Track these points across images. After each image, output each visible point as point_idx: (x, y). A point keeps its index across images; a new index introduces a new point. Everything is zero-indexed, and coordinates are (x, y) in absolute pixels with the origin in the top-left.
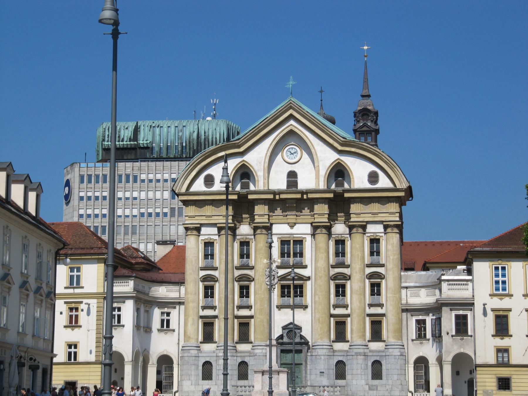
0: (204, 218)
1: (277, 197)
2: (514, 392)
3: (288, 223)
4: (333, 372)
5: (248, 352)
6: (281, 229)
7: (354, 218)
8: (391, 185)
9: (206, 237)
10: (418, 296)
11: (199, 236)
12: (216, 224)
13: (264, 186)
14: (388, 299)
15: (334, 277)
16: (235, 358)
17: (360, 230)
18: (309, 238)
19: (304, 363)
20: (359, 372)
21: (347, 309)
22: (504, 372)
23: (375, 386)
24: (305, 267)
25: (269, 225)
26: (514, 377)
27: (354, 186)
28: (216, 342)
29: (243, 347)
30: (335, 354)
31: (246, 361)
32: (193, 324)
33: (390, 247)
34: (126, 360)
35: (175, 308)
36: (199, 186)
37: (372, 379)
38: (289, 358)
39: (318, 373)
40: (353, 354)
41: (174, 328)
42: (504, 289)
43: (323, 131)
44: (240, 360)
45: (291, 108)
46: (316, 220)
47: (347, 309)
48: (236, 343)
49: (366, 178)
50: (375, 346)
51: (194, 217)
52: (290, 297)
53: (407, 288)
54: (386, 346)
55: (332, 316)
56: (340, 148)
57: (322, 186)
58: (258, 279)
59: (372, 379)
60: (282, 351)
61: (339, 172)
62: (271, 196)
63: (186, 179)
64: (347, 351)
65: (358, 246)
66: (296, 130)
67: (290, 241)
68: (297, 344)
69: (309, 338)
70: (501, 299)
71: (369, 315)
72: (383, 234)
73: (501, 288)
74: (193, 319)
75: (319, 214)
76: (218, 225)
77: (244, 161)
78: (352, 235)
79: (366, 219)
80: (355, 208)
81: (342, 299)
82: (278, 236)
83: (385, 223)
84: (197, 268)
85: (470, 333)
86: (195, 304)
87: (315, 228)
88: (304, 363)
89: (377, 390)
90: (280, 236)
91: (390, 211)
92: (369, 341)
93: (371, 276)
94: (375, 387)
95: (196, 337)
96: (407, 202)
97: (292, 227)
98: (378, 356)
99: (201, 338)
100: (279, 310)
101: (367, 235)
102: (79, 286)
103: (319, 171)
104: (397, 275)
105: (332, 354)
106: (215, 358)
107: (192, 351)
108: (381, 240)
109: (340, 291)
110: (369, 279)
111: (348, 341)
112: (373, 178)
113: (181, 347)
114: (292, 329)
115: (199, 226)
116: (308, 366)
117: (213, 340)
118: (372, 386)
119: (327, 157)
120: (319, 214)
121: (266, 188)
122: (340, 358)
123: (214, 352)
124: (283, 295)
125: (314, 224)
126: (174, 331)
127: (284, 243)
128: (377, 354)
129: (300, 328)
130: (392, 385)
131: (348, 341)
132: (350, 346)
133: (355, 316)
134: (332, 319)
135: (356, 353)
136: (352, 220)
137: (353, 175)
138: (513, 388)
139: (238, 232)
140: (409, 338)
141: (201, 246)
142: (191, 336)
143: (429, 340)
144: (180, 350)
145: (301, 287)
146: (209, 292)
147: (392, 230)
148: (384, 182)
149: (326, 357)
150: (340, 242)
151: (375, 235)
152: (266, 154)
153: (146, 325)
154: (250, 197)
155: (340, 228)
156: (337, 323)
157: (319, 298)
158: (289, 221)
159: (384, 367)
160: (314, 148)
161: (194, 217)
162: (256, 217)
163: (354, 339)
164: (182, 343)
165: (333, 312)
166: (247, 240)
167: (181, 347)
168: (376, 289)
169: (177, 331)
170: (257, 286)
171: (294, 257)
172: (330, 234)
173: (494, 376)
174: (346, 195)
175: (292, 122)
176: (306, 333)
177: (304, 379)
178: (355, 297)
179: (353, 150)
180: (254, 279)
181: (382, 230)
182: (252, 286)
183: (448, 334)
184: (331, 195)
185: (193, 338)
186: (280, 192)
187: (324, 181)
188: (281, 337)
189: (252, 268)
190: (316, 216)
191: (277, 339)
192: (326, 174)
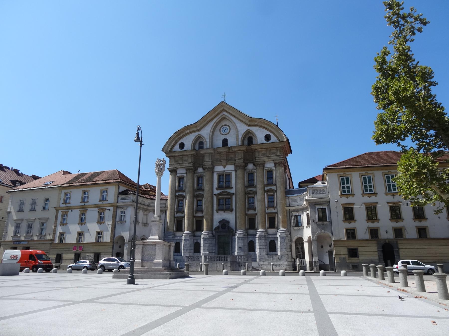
2: (360, 258)
4: (247, 248)
6: (219, 168)
7: (257, 160)
9: (180, 175)
18: (234, 173)
19: (230, 242)
21: (255, 211)
22: (353, 244)
26: (359, 248)
33: (278, 175)
34: (125, 241)
42: (349, 191)
43: (240, 115)
48: (195, 231)
51: (173, 164)
55: (246, 214)
60: (218, 235)
63: (169, 145)
66: (226, 117)
70: (347, 198)
71: (268, 213)
72: (274, 168)
73: (346, 191)
75: (238, 159)
80: (257, 155)
85: (328, 220)
87: (236, 167)
88: (230, 242)
92: (268, 228)
93: (268, 191)
95: (172, 229)
96: (289, 155)
97: (224, 168)
100: (217, 212)
102: (106, 200)
105: (246, 237)
107: (169, 237)
112: (268, 138)
114: (224, 224)
119: (243, 129)
120: (238, 159)
122: (251, 239)
125: (236, 165)
129: (228, 222)
133: (259, 214)
138: (360, 256)
139: (196, 172)
150: (251, 175)
153: (145, 222)
155: (250, 166)
156: (250, 219)
158: (223, 164)
161: (173, 164)
162: (205, 163)
164: (165, 232)
165: (247, 212)
173: (346, 248)
175: (224, 113)
177: (230, 252)
178: (258, 203)
179: (256, 124)
181: (274, 166)
182: (204, 199)
183: (314, 221)
186: (217, 149)
188: (218, 228)
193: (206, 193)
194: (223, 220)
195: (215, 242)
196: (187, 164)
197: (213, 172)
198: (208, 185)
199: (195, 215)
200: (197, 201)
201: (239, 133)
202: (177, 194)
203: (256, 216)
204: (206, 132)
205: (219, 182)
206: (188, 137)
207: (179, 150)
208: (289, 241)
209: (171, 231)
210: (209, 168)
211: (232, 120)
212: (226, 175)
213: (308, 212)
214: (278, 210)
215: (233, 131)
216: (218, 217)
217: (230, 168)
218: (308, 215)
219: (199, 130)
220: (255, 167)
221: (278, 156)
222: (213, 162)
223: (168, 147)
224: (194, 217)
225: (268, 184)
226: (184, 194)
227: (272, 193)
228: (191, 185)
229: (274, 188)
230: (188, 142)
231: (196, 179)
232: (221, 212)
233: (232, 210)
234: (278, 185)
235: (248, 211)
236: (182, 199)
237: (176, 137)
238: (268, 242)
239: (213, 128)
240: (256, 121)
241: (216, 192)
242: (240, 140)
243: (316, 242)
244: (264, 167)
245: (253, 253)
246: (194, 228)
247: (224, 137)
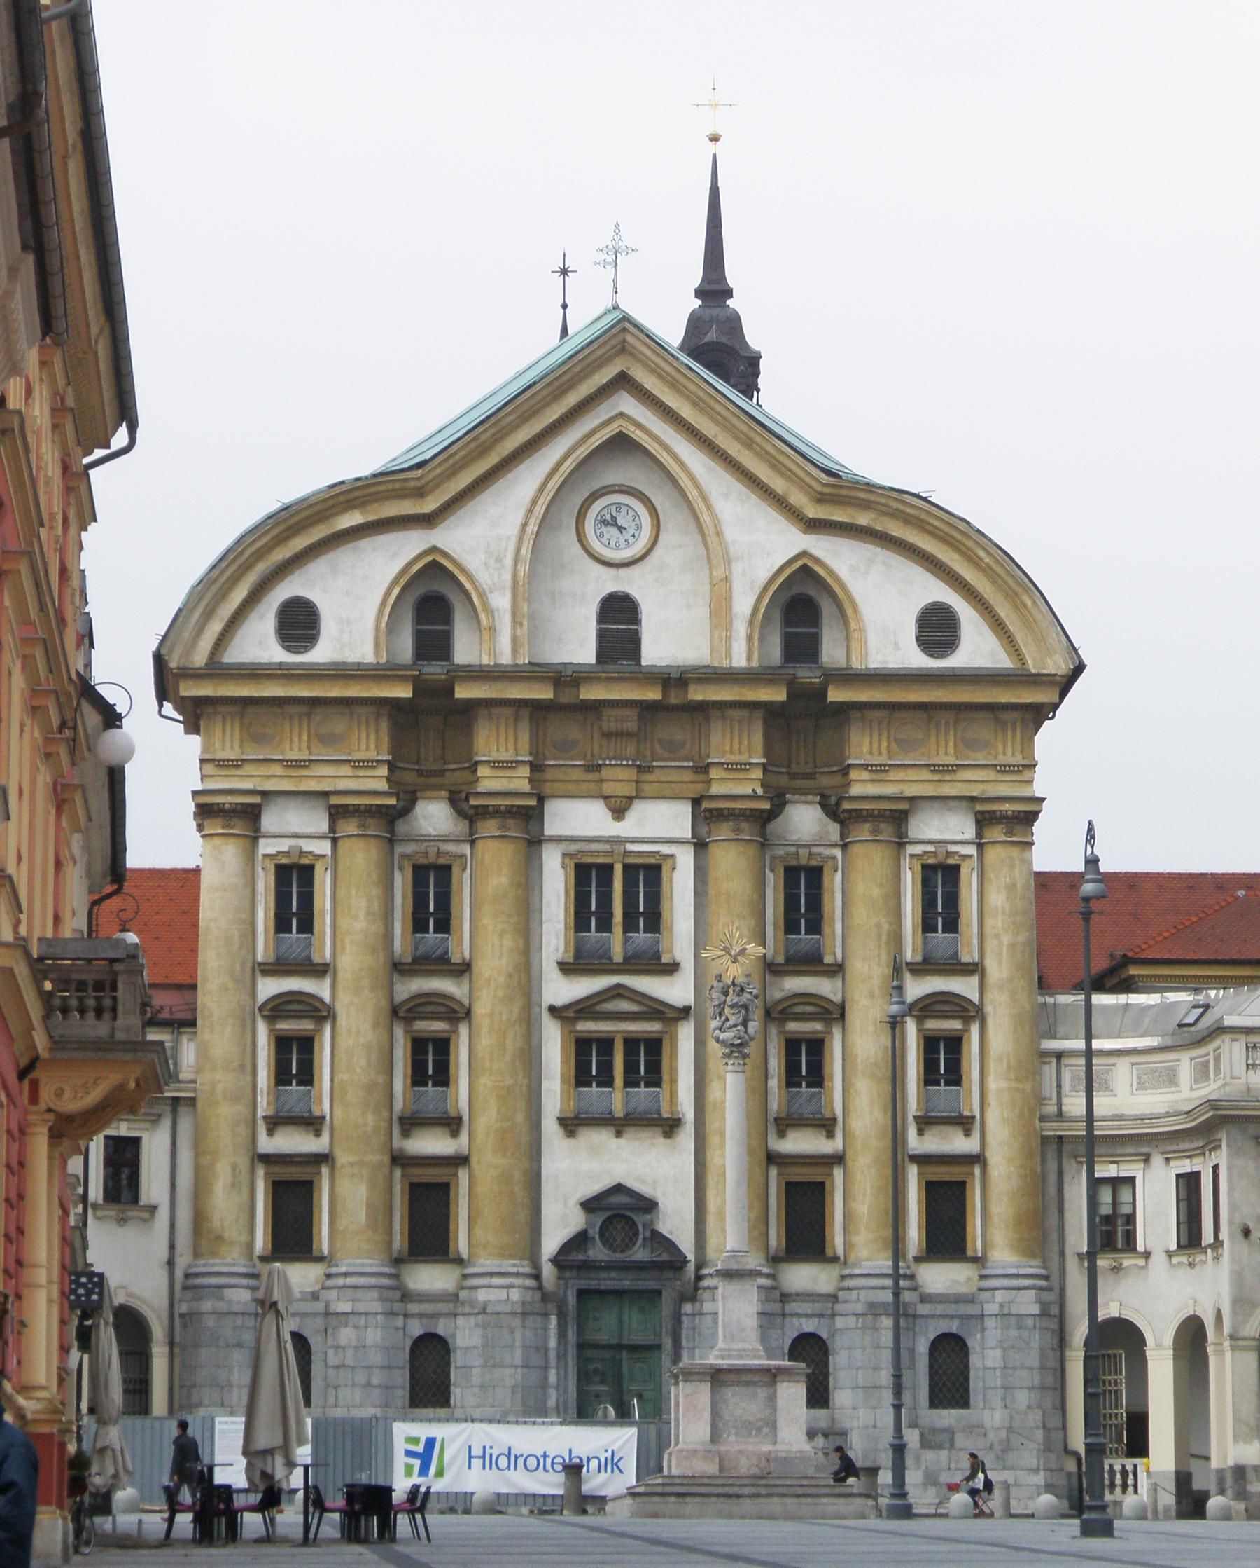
0: (278, 770)
1: (566, 697)
3: (606, 798)
5: (454, 1297)
6: (578, 819)
8: (1004, 661)
9: (284, 845)
11: (255, 839)
12: (326, 794)
13: (515, 651)
14: (992, 1099)
15: (782, 1011)
16: (400, 1321)
17: (887, 832)
18: (685, 859)
19: (668, 1343)
21: (830, 1135)
23: (944, 1430)
24: (672, 968)
25: (533, 802)
27: (865, 657)
28: (321, 1259)
29: (430, 1278)
30: (792, 1307)
31: (441, 1331)
32: (233, 1186)
33: (997, 899)
35: (155, 1120)
36: (260, 642)
37: (935, 1402)
38: (606, 1326)
40: (859, 1308)
41: (153, 1201)
43: (748, 443)
44: (416, 1329)
45: (623, 349)
46: (715, 789)
47: (830, 1135)
48: (398, 1261)
49: (911, 630)
50: (941, 1277)
51: (238, 764)
52: (607, 1081)
53: (1059, 1055)
55: (772, 1158)
56: (813, 511)
57: (739, 658)
58: (491, 1015)
59: (935, 1402)
60: (581, 1294)
61: (801, 604)
62: (544, 693)
63: (209, 614)
64: (834, 1298)
65: (876, 892)
66: (638, 435)
67: (609, 868)
68: (640, 1267)
69: (686, 1244)
72: (971, 850)
74: (234, 1167)
76: (334, 800)
77: (434, 549)
78: (855, 849)
79: (911, 791)
80: (863, 746)
81: (813, 1095)
82: (563, 847)
83: (979, 807)
84: (249, 964)
86: (242, 1109)
88: (668, 1343)
89: (952, 1445)
90: (573, 848)
91: (1002, 759)
92: (918, 1259)
94: (945, 1436)
95: (244, 1238)
97: (619, 812)
98: (952, 1317)
99: (261, 1242)
101: (911, 849)
103: (728, 598)
104: (1028, 1007)
105: (776, 1307)
106: (319, 1322)
107: (228, 1293)
108: (964, 871)
109: (806, 1063)
110: (920, 1019)
111: (835, 1259)
112: (937, 629)
113: (179, 1274)
114: (619, 1211)
115: (256, 800)
116: (685, 1353)
117: (310, 1249)
118: (934, 1431)
121: (523, 660)
122: (809, 1326)
123: (315, 1296)
124: (581, 1076)
125: (706, 805)
126: (153, 1209)
127: (589, 876)
128: (952, 1309)
129: (649, 1206)
130: (1010, 1430)
131: (835, 1259)
134: (774, 1172)
135: (872, 1305)
136: (855, 790)
137: (858, 618)
139: (401, 827)
140: (1069, 1252)
141: (265, 883)
142: (226, 1235)
143: (1147, 1255)
144: (178, 1287)
145: (654, 1046)
146: (294, 1061)
147: (1010, 833)
148: (977, 648)
151: (942, 851)
152: (524, 526)
154: (463, 692)
155: (804, 821)
158: (608, 788)
159: (975, 1360)
160: (709, 507)
161: (238, 764)
162: (482, 771)
163: (864, 1253)
164: (182, 1262)
166: (442, 861)
167: (179, 1274)
168: (944, 1061)
169: (163, 1215)
170: (485, 1041)
171: (626, 930)
172: (764, 844)
174: (836, 695)
175: (626, 403)
176: (676, 1221)
179: (863, 519)
180: (468, 1013)
181: (970, 832)
184: (778, 695)
185: (232, 1243)
187: (750, 638)
188: (579, 1241)
189: (463, 970)
190: (714, 773)
191: (567, 1247)
192: (755, 611)
193: (488, 995)
194: (619, 1189)
195: (562, 1335)
196: (345, 770)
197: (535, 842)
198: (508, 942)
199: (398, 1142)
200: (419, 1045)
201: (737, 568)
202: (269, 987)
203: (838, 1173)
204: (484, 540)
205: (580, 919)
206: (344, 556)
207: (276, 654)
208: (1056, 1341)
209: (232, 1260)
210: (512, 812)
211: (682, 464)
212: (631, 870)
213: (1186, 1166)
214: (992, 1141)
215: (677, 545)
216: (576, 1170)
217: (660, 823)
218: (1189, 1185)
219: (428, 520)
220: (834, 830)
221: (1004, 769)
222: (536, 767)
223: (199, 632)
224: (398, 1159)
225: (926, 967)
226: (321, 989)
227: (956, 1025)
228: (378, 927)
229: (965, 987)
230: (355, 603)
231: (402, 883)
232: (601, 1137)
233: (670, 1126)
234: (997, 969)
235: (782, 1134)
236: (307, 1025)
237: (260, 554)
238: (923, 1347)
239: (540, 509)
240: (865, 505)
241: (563, 990)
242: (740, 629)
244: (900, 842)
245: (824, 1412)
246: (399, 1241)
247: (610, 582)
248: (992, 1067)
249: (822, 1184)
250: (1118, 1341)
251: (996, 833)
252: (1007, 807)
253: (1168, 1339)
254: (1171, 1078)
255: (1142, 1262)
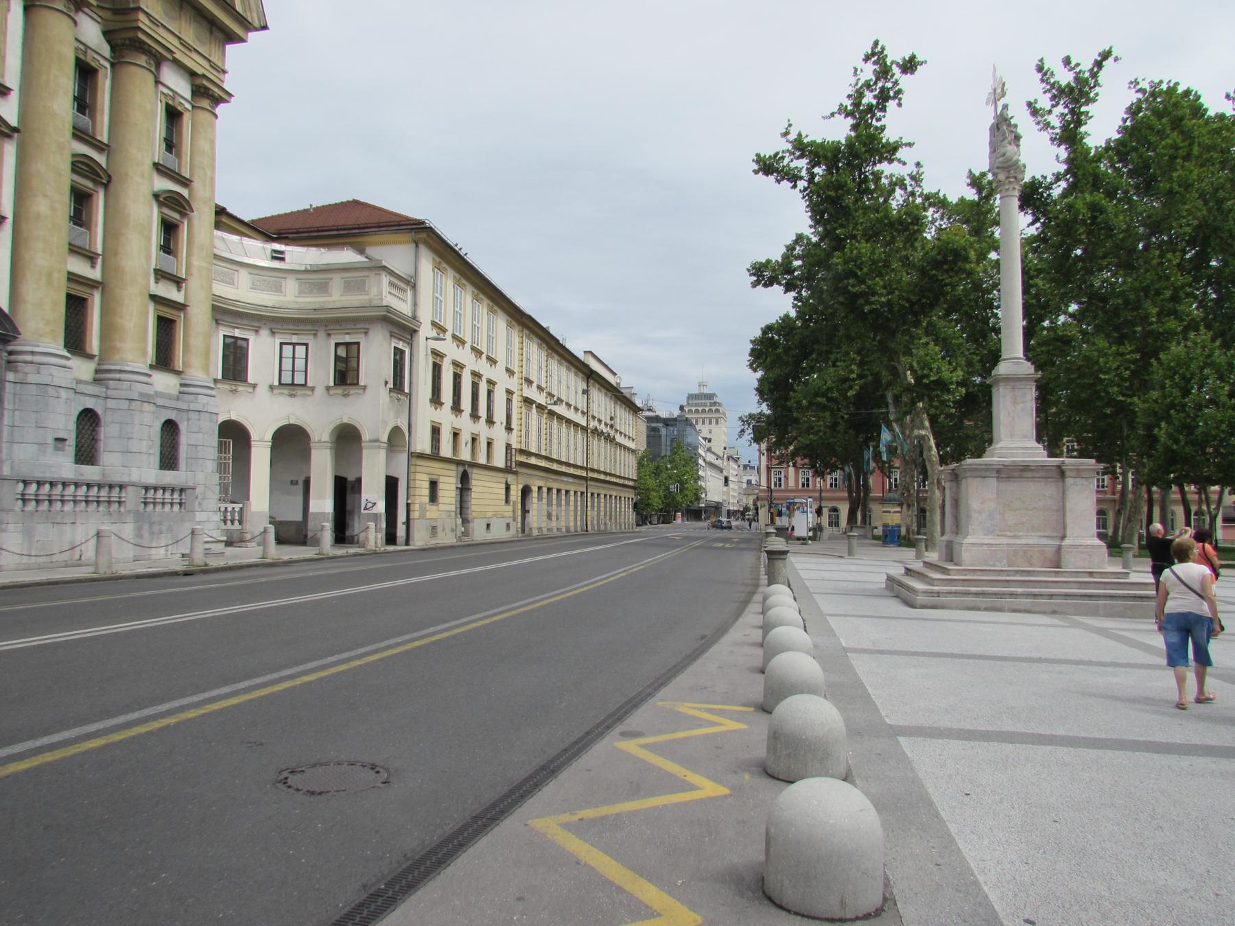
2: (442, 507)
10: (231, 282)
14: (195, 271)
20: (144, 446)
21: (93, 266)
26: (442, 479)
39: (50, 440)
47: (93, 266)
50: (164, 382)
54: (182, 385)
101: (161, 88)
110: (161, 204)
111: (91, 357)
122: (90, 404)
131: (91, 357)
132: (97, 371)
135: (141, 394)
149: (71, 394)
157: (53, 209)
220: (106, 50)
243: (382, 454)
248: (195, 251)
249: (85, 300)
250: (234, 436)
251: (206, 103)
252: (216, 90)
253: (269, 436)
254: (278, 289)
255: (251, 390)
